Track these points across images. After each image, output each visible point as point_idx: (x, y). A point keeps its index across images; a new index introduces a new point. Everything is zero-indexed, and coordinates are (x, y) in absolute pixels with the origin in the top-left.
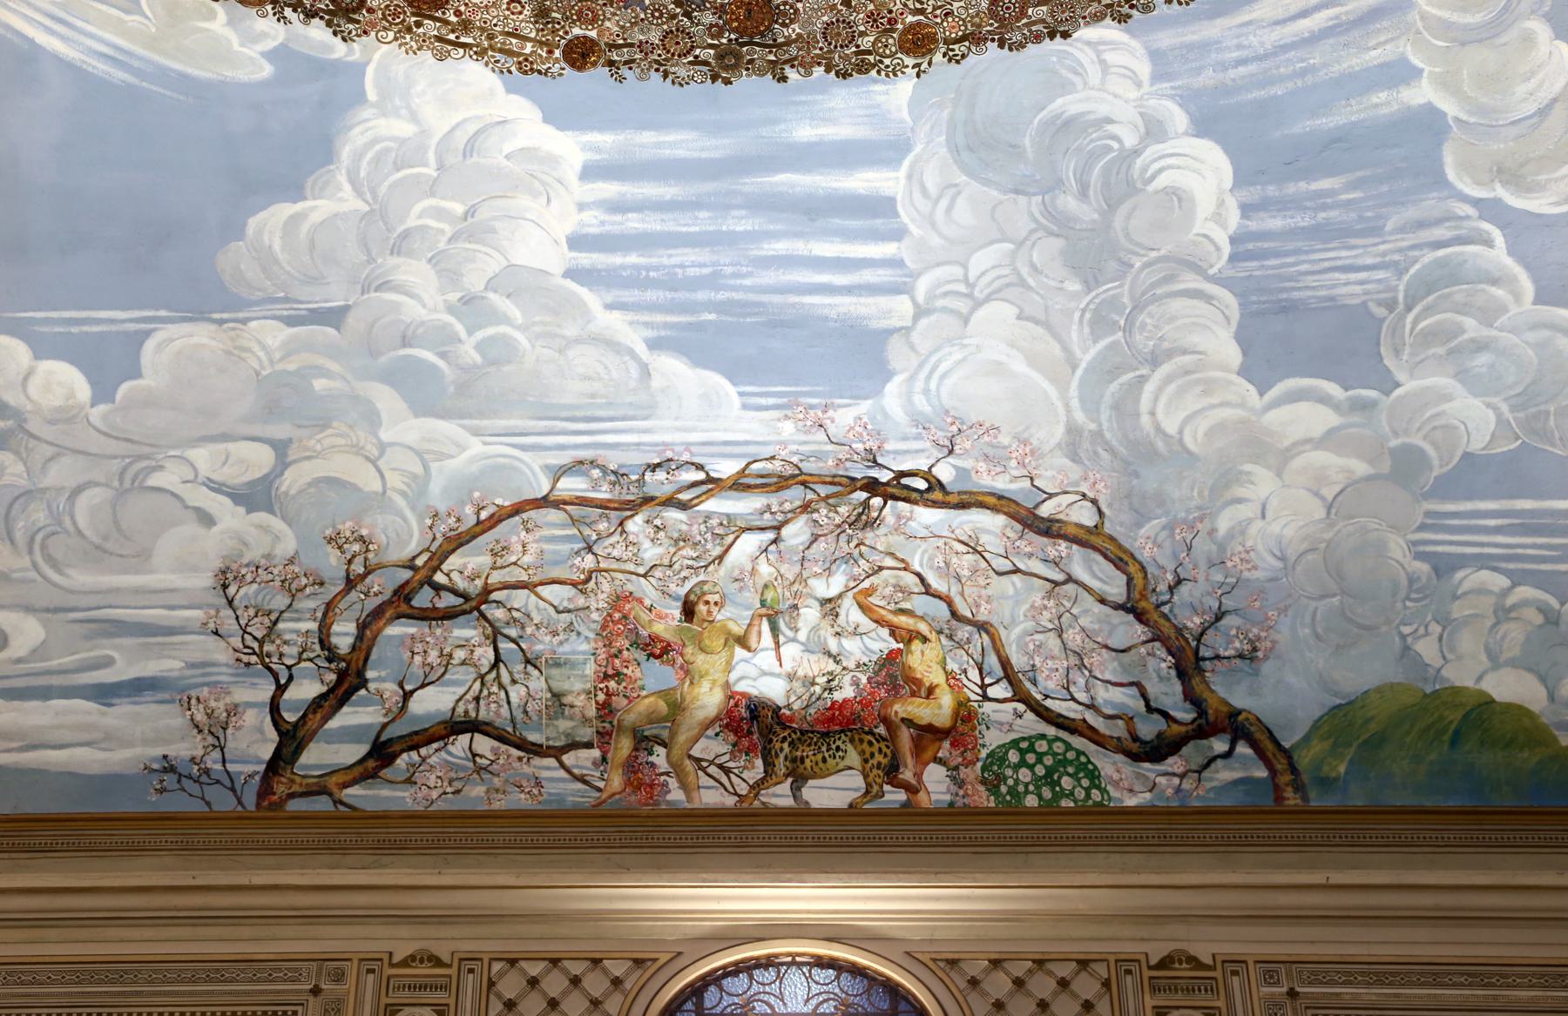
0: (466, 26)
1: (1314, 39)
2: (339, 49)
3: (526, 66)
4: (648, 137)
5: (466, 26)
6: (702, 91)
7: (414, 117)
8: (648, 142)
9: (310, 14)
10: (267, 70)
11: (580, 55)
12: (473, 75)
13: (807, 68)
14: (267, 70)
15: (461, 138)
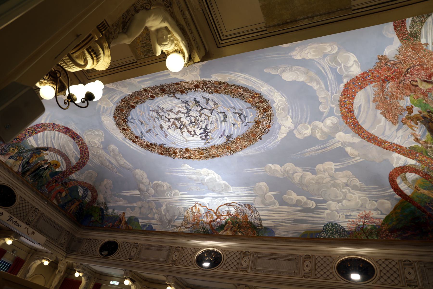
0: (191, 84)
1: (112, 96)
2: (204, 79)
3: (183, 82)
4: (165, 79)
5: (191, 84)
6: (163, 83)
7: (192, 75)
8: (165, 78)
9: (209, 81)
10: (212, 76)
11: (177, 84)
12: (188, 80)
13: (154, 87)
14: (212, 76)
15: (186, 74)
